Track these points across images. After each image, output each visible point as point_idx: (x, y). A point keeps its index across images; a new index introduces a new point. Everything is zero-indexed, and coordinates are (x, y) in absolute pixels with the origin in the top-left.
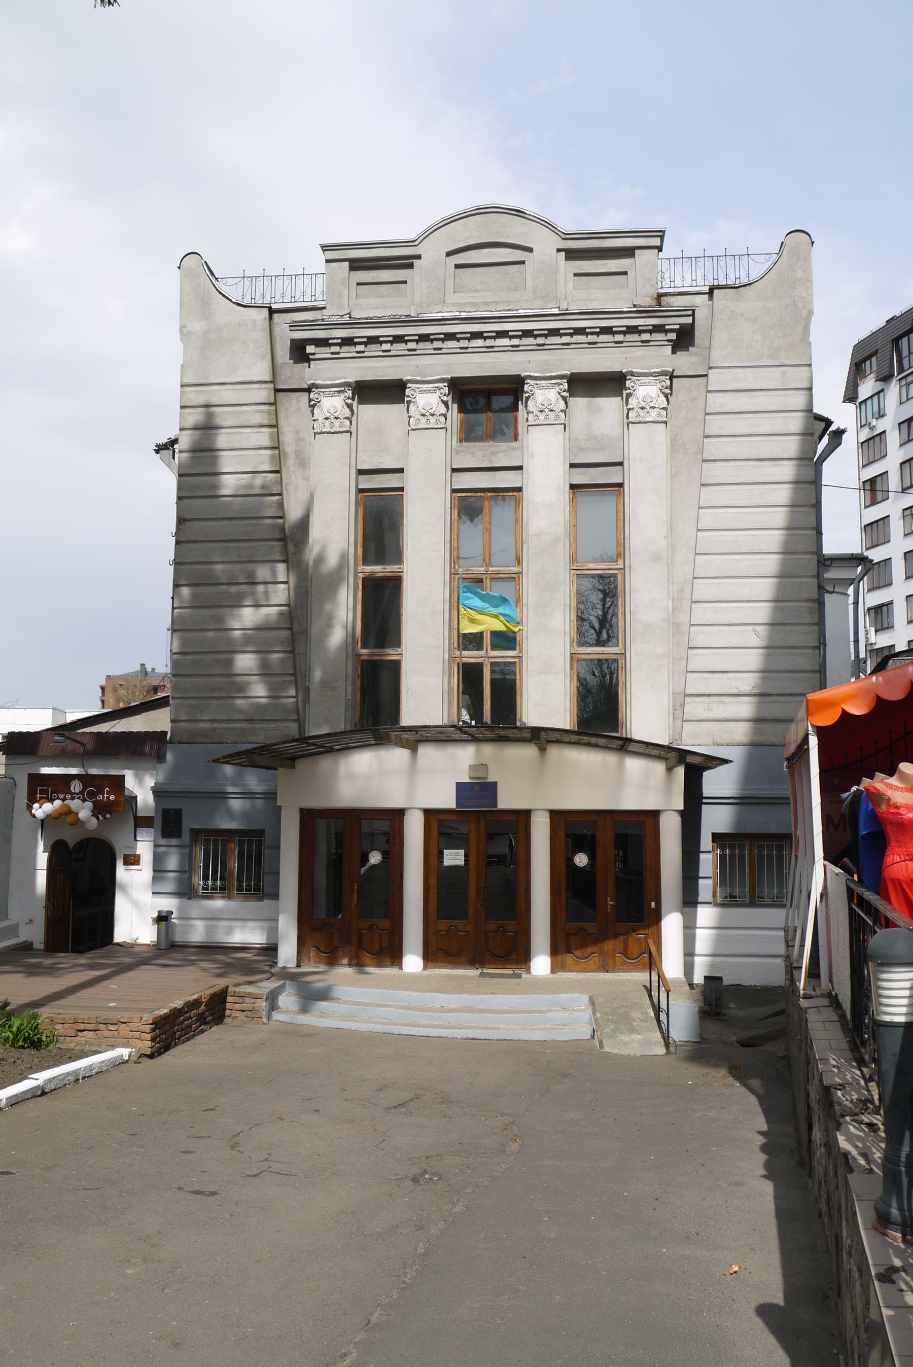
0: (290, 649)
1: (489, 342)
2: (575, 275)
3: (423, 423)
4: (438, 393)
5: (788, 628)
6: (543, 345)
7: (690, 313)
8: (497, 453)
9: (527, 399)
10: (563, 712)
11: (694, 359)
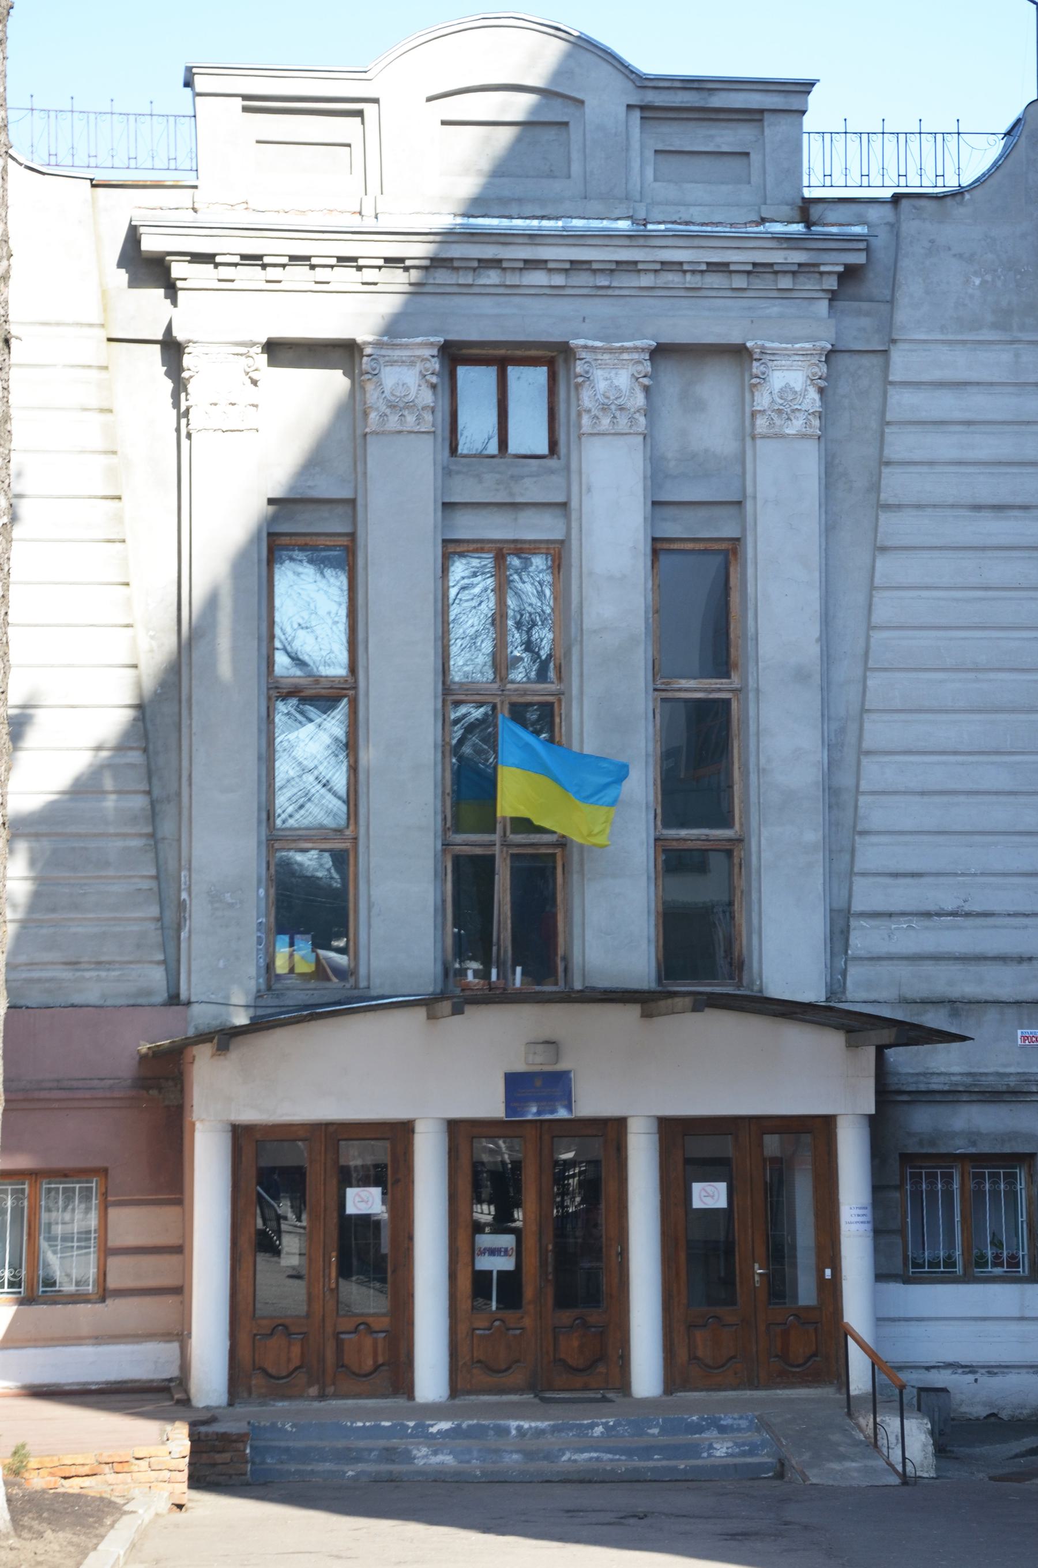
0: (149, 830)
1: (512, 279)
2: (656, 151)
3: (393, 422)
4: (419, 366)
5: (1022, 799)
6: (609, 287)
7: (862, 245)
8: (523, 477)
9: (578, 386)
10: (644, 945)
11: (865, 322)
